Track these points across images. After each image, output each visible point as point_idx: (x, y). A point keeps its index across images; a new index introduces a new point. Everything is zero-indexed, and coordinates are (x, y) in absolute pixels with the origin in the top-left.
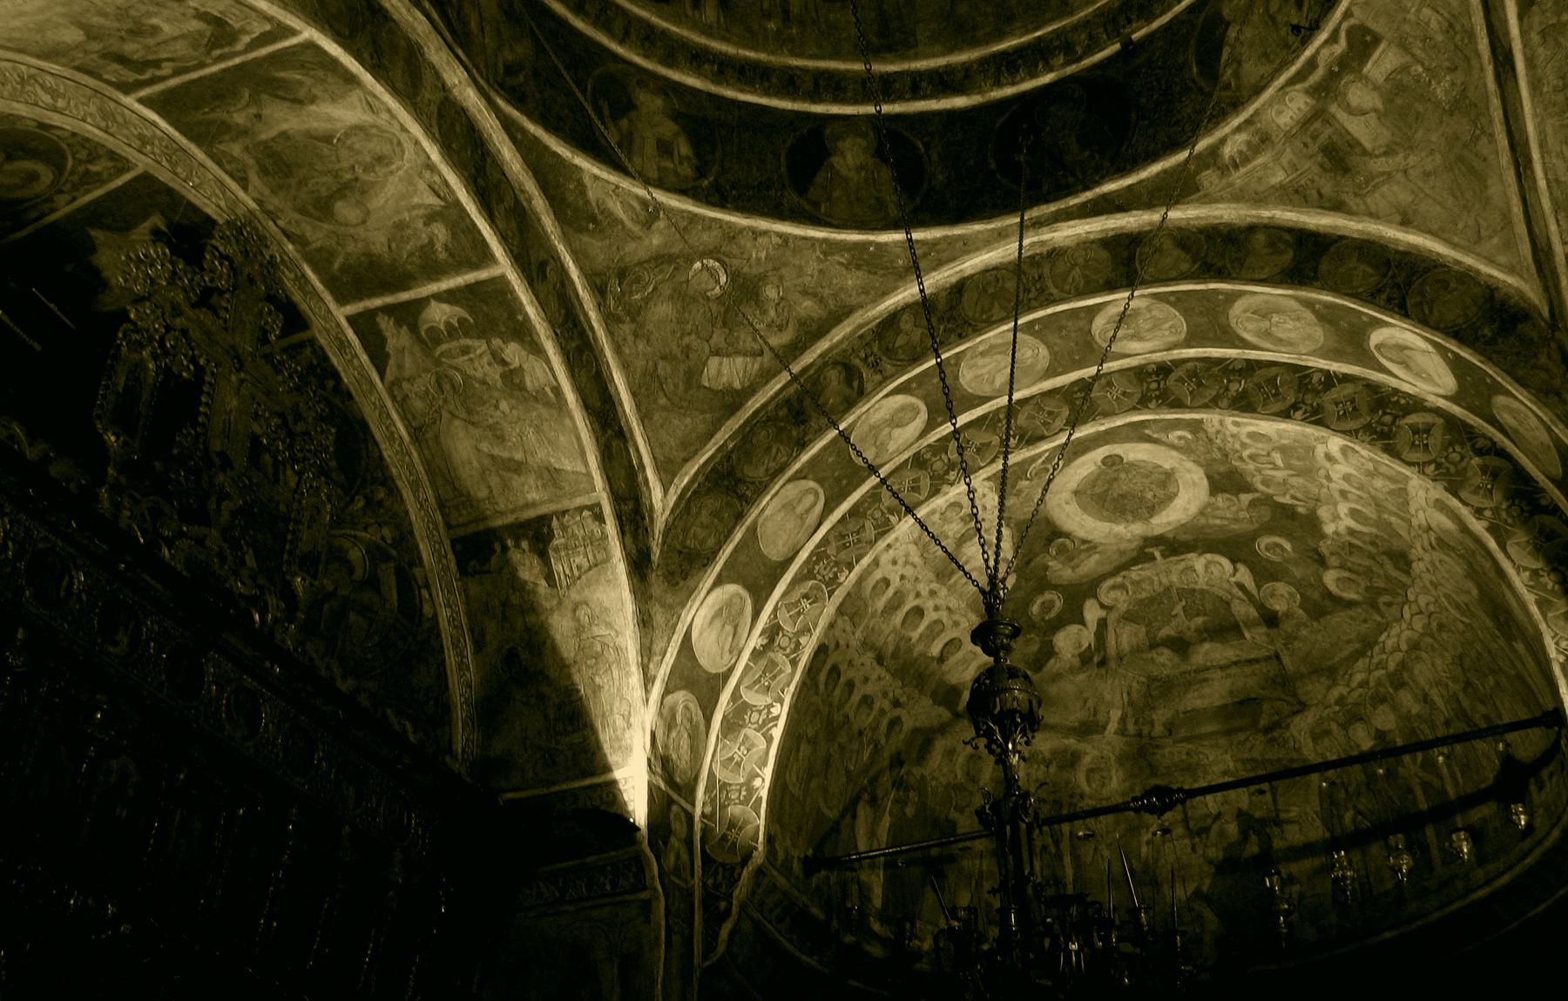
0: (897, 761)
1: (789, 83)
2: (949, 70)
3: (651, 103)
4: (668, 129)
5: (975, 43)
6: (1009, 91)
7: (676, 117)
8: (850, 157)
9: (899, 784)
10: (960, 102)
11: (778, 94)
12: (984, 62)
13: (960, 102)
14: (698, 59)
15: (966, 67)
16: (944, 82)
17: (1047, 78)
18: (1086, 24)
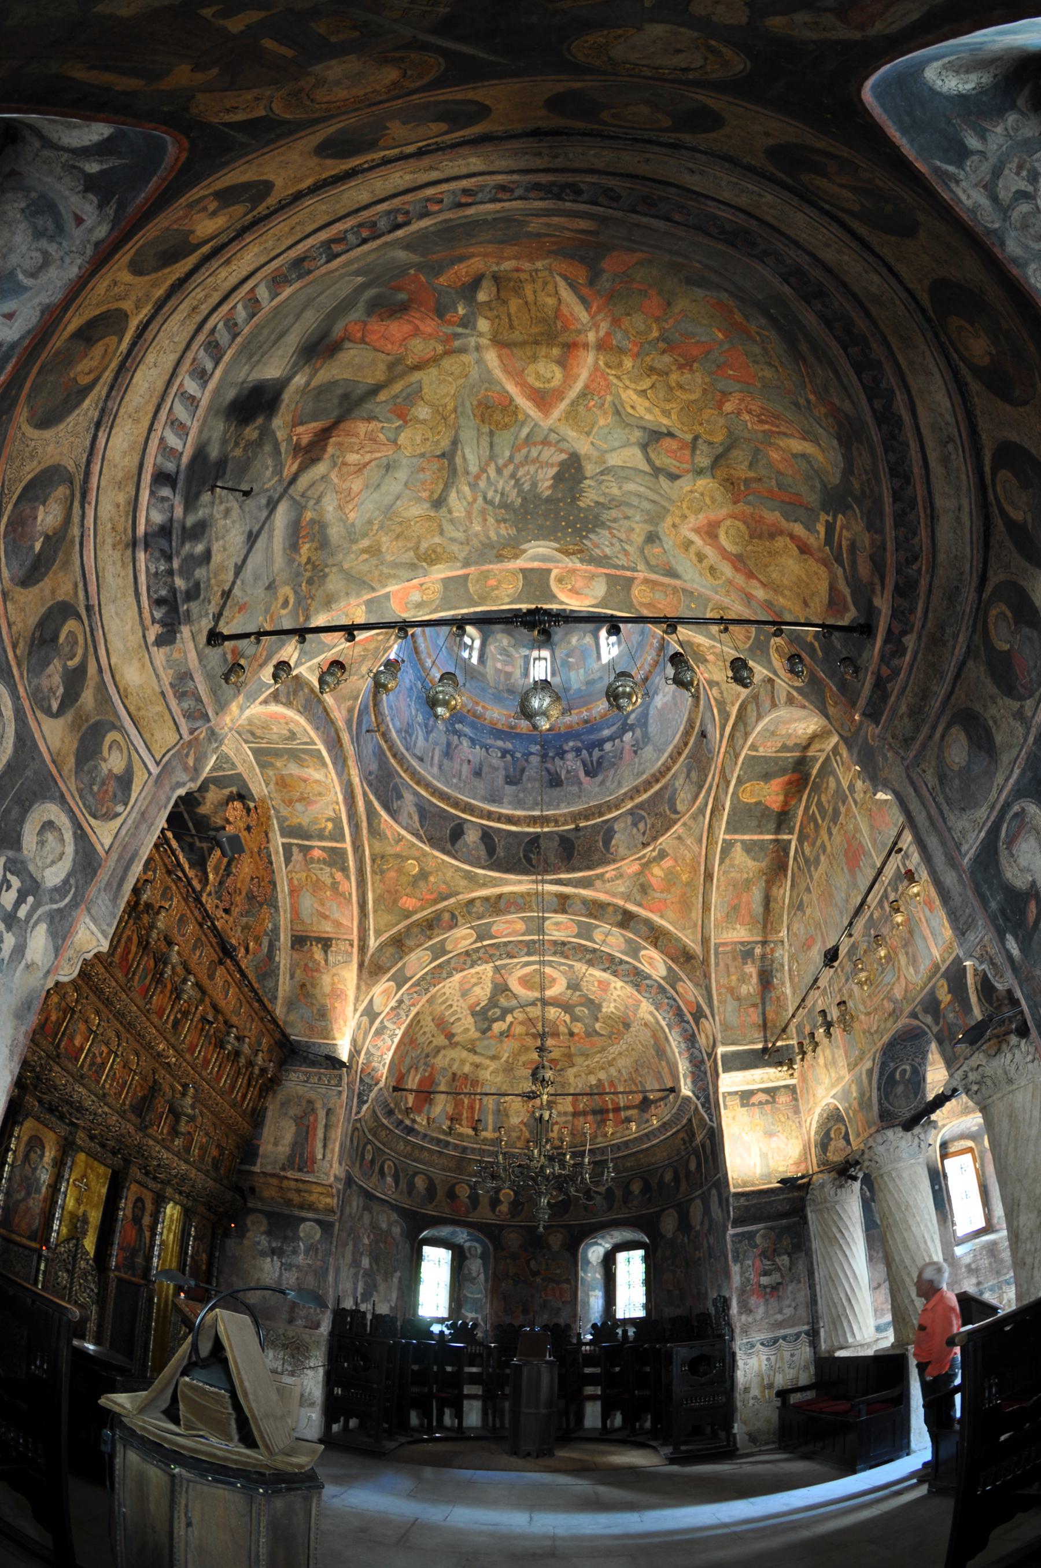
0: (427, 1056)
1: (456, 804)
2: (513, 816)
3: (408, 797)
4: (413, 810)
5: (525, 809)
6: (531, 830)
7: (416, 805)
8: (472, 837)
9: (425, 1064)
10: (513, 828)
11: (451, 806)
12: (525, 817)
13: (513, 828)
14: (427, 786)
15: (519, 817)
16: (510, 820)
17: (546, 830)
18: (565, 815)
